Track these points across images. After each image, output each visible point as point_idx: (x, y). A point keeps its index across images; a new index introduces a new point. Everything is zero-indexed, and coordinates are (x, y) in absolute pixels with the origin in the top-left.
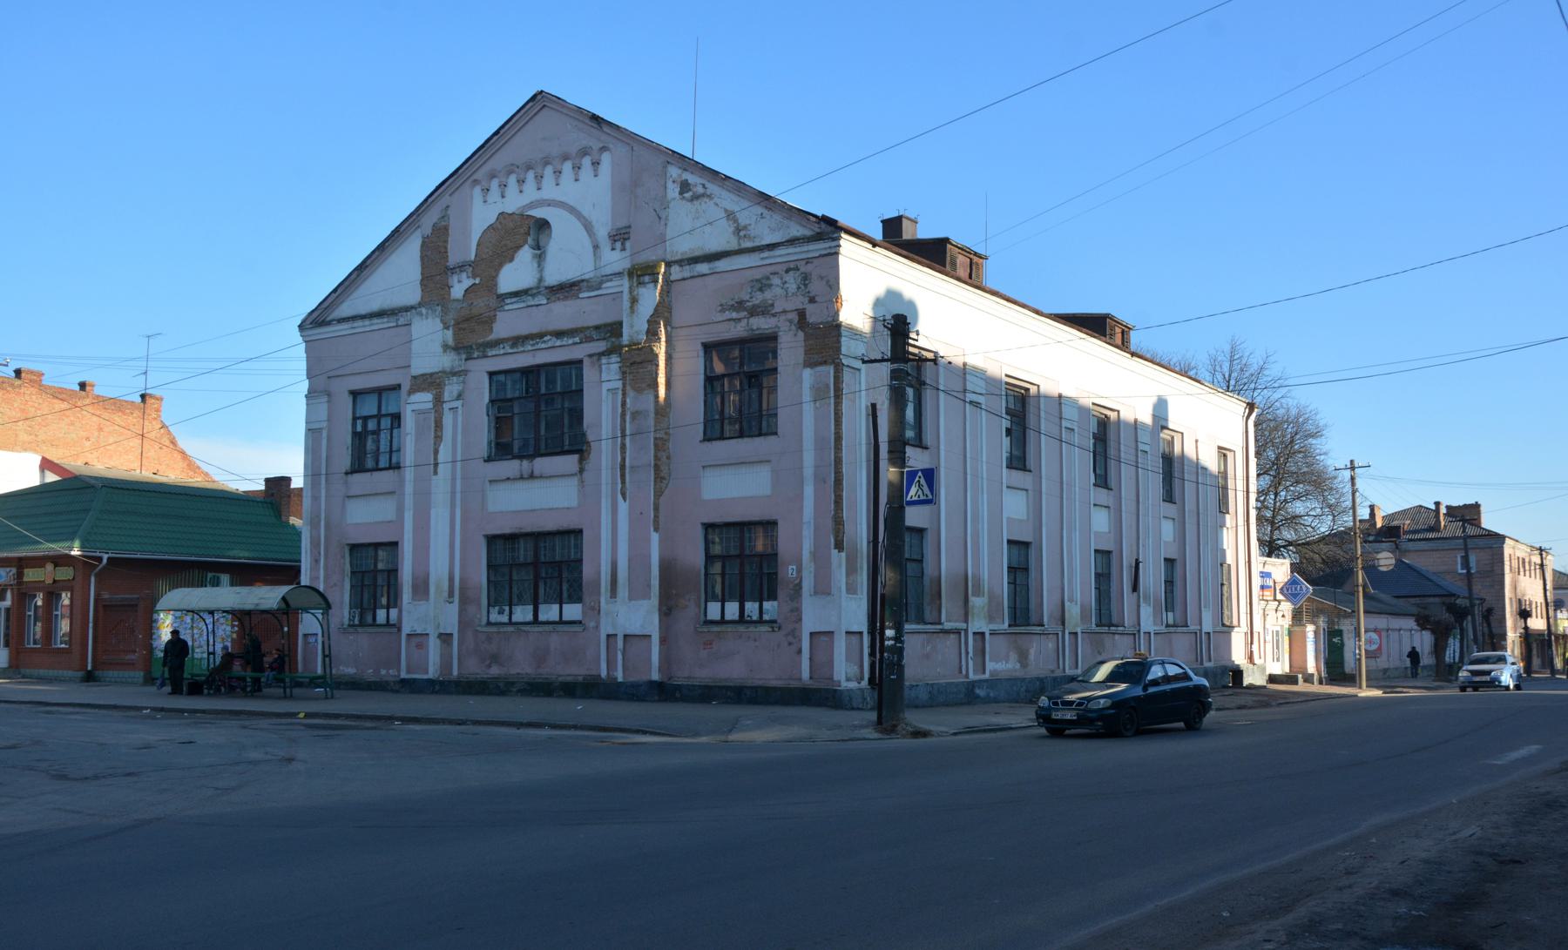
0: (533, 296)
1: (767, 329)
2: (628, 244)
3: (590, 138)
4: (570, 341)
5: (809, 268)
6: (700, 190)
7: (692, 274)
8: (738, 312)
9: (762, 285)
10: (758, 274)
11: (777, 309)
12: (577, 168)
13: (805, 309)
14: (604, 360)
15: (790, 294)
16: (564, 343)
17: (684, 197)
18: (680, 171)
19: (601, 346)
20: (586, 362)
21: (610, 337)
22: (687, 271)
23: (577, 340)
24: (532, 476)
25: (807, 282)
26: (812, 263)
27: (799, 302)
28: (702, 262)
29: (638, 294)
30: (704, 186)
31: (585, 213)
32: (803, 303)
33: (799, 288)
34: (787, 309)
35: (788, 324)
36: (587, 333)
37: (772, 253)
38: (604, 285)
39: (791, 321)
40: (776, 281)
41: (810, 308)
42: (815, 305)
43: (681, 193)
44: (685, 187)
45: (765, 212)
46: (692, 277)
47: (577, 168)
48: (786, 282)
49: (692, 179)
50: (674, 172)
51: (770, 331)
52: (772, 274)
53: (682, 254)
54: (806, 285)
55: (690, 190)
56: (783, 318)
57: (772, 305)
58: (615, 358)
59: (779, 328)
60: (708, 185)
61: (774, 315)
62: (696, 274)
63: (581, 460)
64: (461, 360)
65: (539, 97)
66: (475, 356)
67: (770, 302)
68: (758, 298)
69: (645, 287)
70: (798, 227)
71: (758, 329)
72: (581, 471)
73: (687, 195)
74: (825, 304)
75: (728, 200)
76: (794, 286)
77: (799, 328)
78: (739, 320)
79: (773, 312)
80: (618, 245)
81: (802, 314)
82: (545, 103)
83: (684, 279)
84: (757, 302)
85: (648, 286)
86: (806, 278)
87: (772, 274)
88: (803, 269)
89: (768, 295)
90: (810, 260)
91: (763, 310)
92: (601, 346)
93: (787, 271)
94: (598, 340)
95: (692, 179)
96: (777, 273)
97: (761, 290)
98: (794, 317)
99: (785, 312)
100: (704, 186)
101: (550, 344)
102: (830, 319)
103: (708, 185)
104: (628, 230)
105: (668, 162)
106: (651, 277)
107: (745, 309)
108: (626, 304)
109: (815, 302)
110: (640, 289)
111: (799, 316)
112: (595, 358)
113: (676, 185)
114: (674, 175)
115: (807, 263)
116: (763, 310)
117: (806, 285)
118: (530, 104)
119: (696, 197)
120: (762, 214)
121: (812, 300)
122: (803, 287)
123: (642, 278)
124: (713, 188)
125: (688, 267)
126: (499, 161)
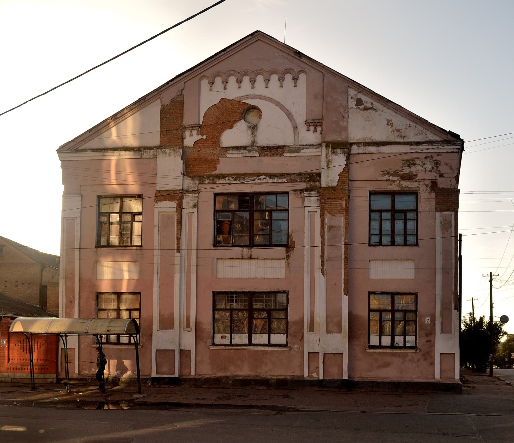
0: (250, 151)
1: (412, 188)
2: (319, 129)
3: (295, 65)
4: (280, 181)
5: (439, 158)
6: (370, 106)
7: (365, 152)
8: (393, 177)
9: (411, 163)
10: (407, 157)
11: (419, 177)
12: (281, 79)
13: (437, 180)
14: (306, 194)
15: (427, 171)
16: (275, 181)
17: (359, 108)
18: (356, 93)
19: (303, 185)
20: (291, 194)
21: (309, 181)
22: (361, 150)
23: (285, 180)
24: (250, 258)
25: (438, 165)
26: (441, 155)
27: (433, 176)
28: (373, 146)
29: (332, 159)
30: (372, 104)
31: (288, 107)
32: (436, 177)
33: (433, 168)
34: (425, 179)
35: (425, 187)
36: (293, 177)
37: (418, 147)
38: (302, 151)
39: (427, 186)
40: (418, 162)
41: (440, 180)
42: (443, 178)
43: (357, 105)
44: (359, 102)
45: (413, 124)
46: (364, 153)
47: (281, 79)
48: (425, 164)
49: (364, 98)
50: (352, 92)
51: (413, 189)
52: (415, 158)
53: (357, 139)
54: (437, 167)
55: (363, 104)
56: (422, 183)
57: (416, 175)
58: (313, 193)
59: (420, 188)
60: (374, 103)
61: (416, 181)
62: (367, 152)
63: (287, 252)
64: (195, 184)
65: (256, 34)
66: (207, 182)
67: (415, 173)
68: (407, 170)
69: (337, 155)
70: (432, 135)
71: (406, 187)
72: (288, 257)
73: (362, 107)
74: (449, 179)
75: (388, 114)
76: (430, 167)
77: (432, 189)
78: (394, 181)
79: (417, 179)
80: (312, 128)
81: (434, 183)
82: (259, 38)
83: (359, 154)
84: (406, 172)
85: (339, 154)
86: (437, 163)
87: (415, 158)
88: (435, 158)
89: (413, 169)
90: (440, 154)
91: (410, 177)
92: (303, 185)
93: (426, 158)
94: (300, 182)
95: (364, 98)
96: (420, 158)
97: (409, 166)
98: (428, 183)
99: (424, 179)
100: (372, 104)
101: (264, 181)
102: (452, 187)
103: (374, 103)
104: (321, 121)
105: (348, 86)
106: (342, 150)
107: (399, 175)
108: (324, 164)
109: (443, 177)
110: (333, 156)
111: (432, 183)
112: (299, 192)
113: (353, 100)
114: (352, 95)
115: (438, 155)
116: (410, 177)
117: (437, 167)
118: (250, 37)
119: (366, 109)
120: (409, 125)
121: (441, 176)
122: (435, 168)
123: (335, 150)
124: (376, 105)
125: (362, 147)
126: (223, 66)
